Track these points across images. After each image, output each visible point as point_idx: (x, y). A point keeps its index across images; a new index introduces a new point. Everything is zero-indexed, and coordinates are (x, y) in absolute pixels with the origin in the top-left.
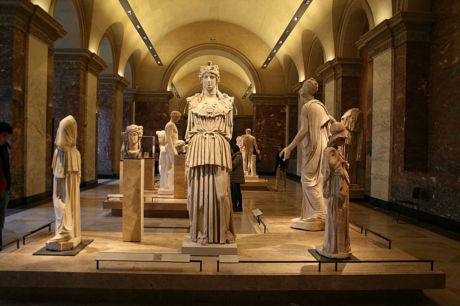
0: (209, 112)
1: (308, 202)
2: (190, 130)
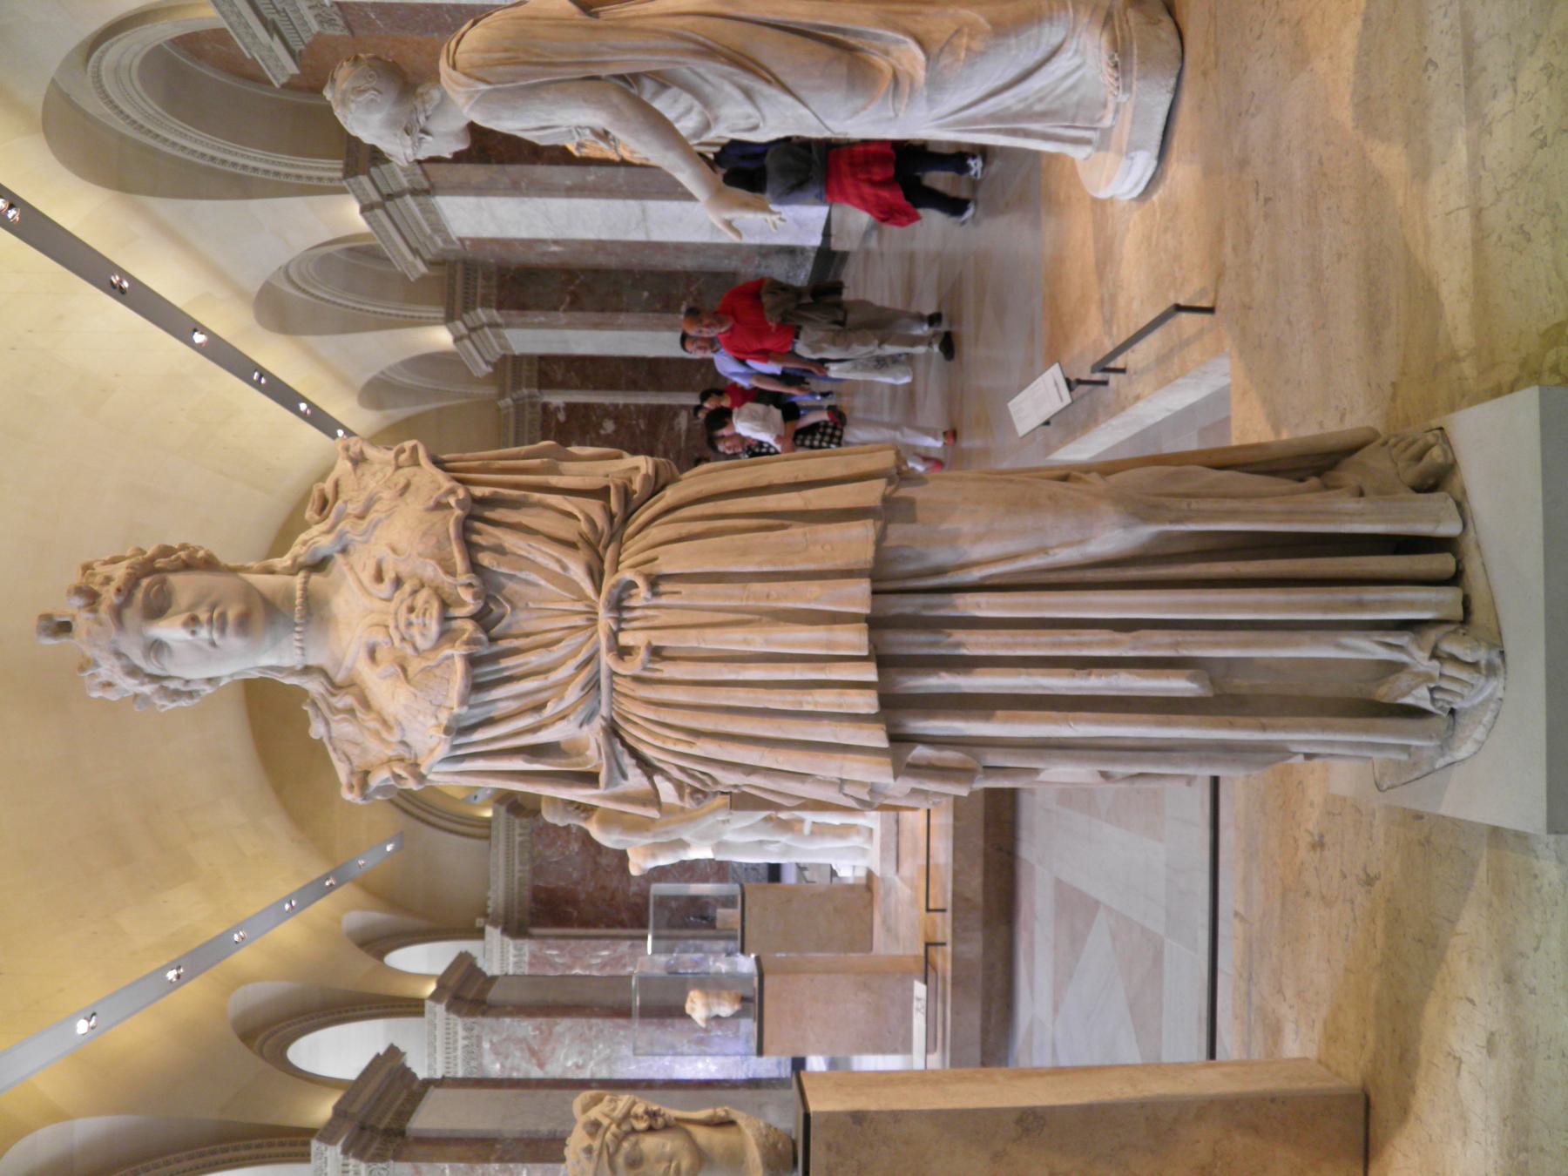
0: (434, 628)
1: (1008, 99)
2: (590, 778)
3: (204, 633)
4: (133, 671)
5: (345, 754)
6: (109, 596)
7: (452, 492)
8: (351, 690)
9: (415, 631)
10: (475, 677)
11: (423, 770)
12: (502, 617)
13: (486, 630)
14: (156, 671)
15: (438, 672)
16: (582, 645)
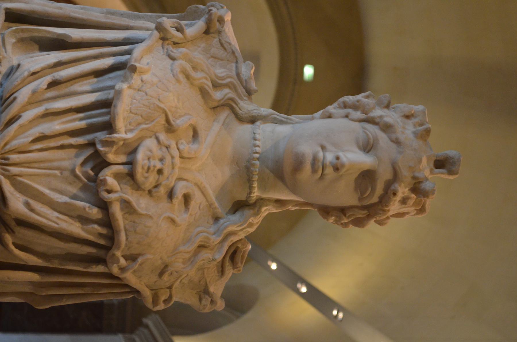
3: (330, 157)
4: (387, 128)
5: (225, 49)
6: (403, 190)
7: (123, 269)
8: (216, 104)
9: (158, 152)
10: (109, 113)
11: (156, 33)
12: (83, 164)
13: (97, 154)
14: (369, 127)
15: (139, 118)
16: (14, 137)
